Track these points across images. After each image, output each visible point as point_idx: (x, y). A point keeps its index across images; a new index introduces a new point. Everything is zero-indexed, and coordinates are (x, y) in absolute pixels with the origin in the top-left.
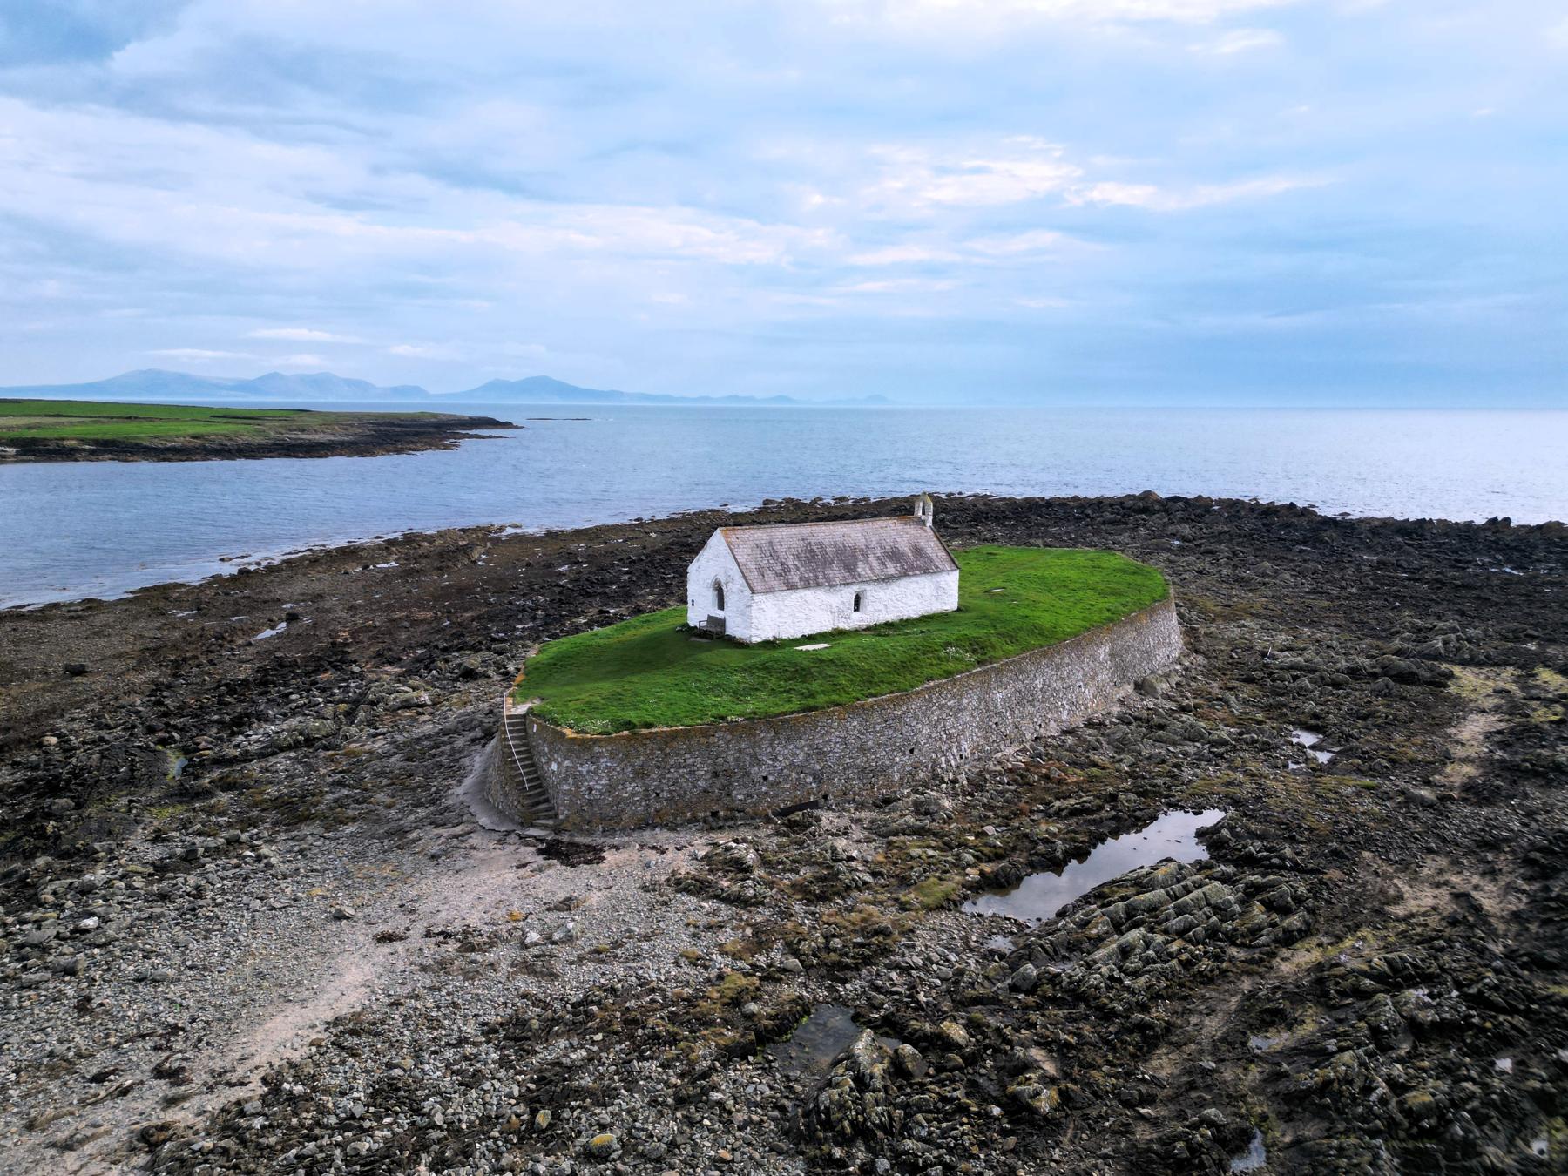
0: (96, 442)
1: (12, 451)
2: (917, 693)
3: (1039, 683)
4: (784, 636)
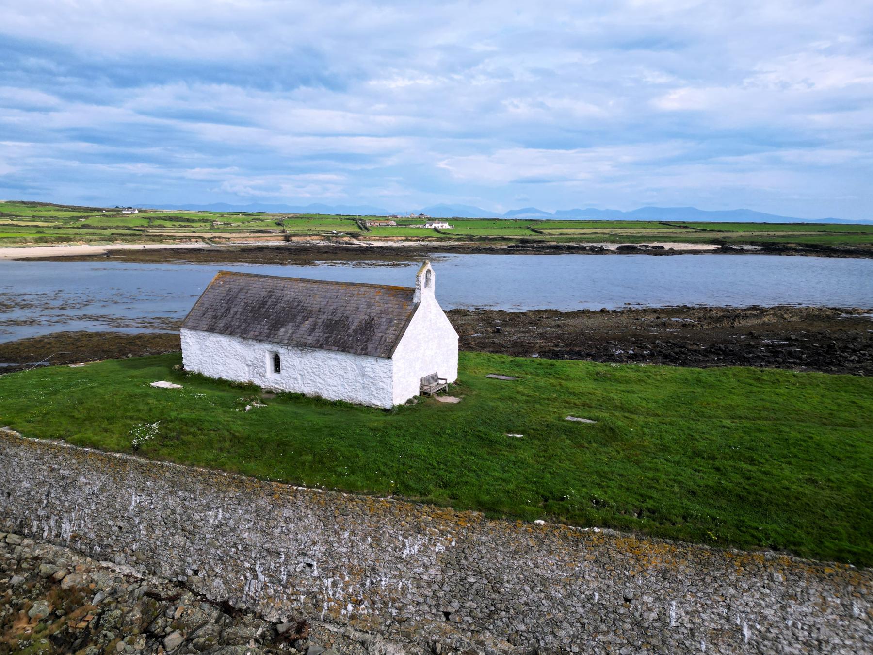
0: (807, 245)
1: (759, 248)
2: (32, 444)
3: (215, 516)
4: (206, 374)
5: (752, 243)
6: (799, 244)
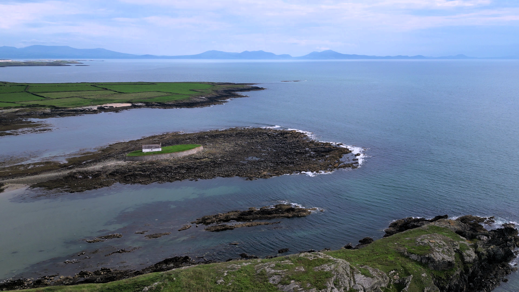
5: (141, 102)
6: (156, 102)
